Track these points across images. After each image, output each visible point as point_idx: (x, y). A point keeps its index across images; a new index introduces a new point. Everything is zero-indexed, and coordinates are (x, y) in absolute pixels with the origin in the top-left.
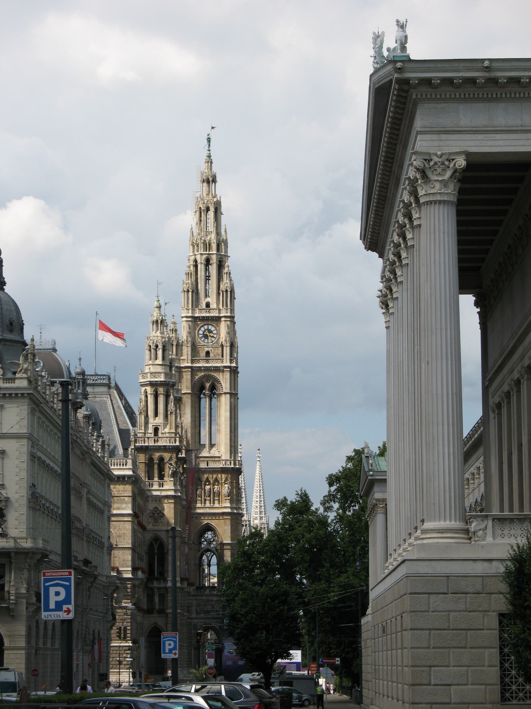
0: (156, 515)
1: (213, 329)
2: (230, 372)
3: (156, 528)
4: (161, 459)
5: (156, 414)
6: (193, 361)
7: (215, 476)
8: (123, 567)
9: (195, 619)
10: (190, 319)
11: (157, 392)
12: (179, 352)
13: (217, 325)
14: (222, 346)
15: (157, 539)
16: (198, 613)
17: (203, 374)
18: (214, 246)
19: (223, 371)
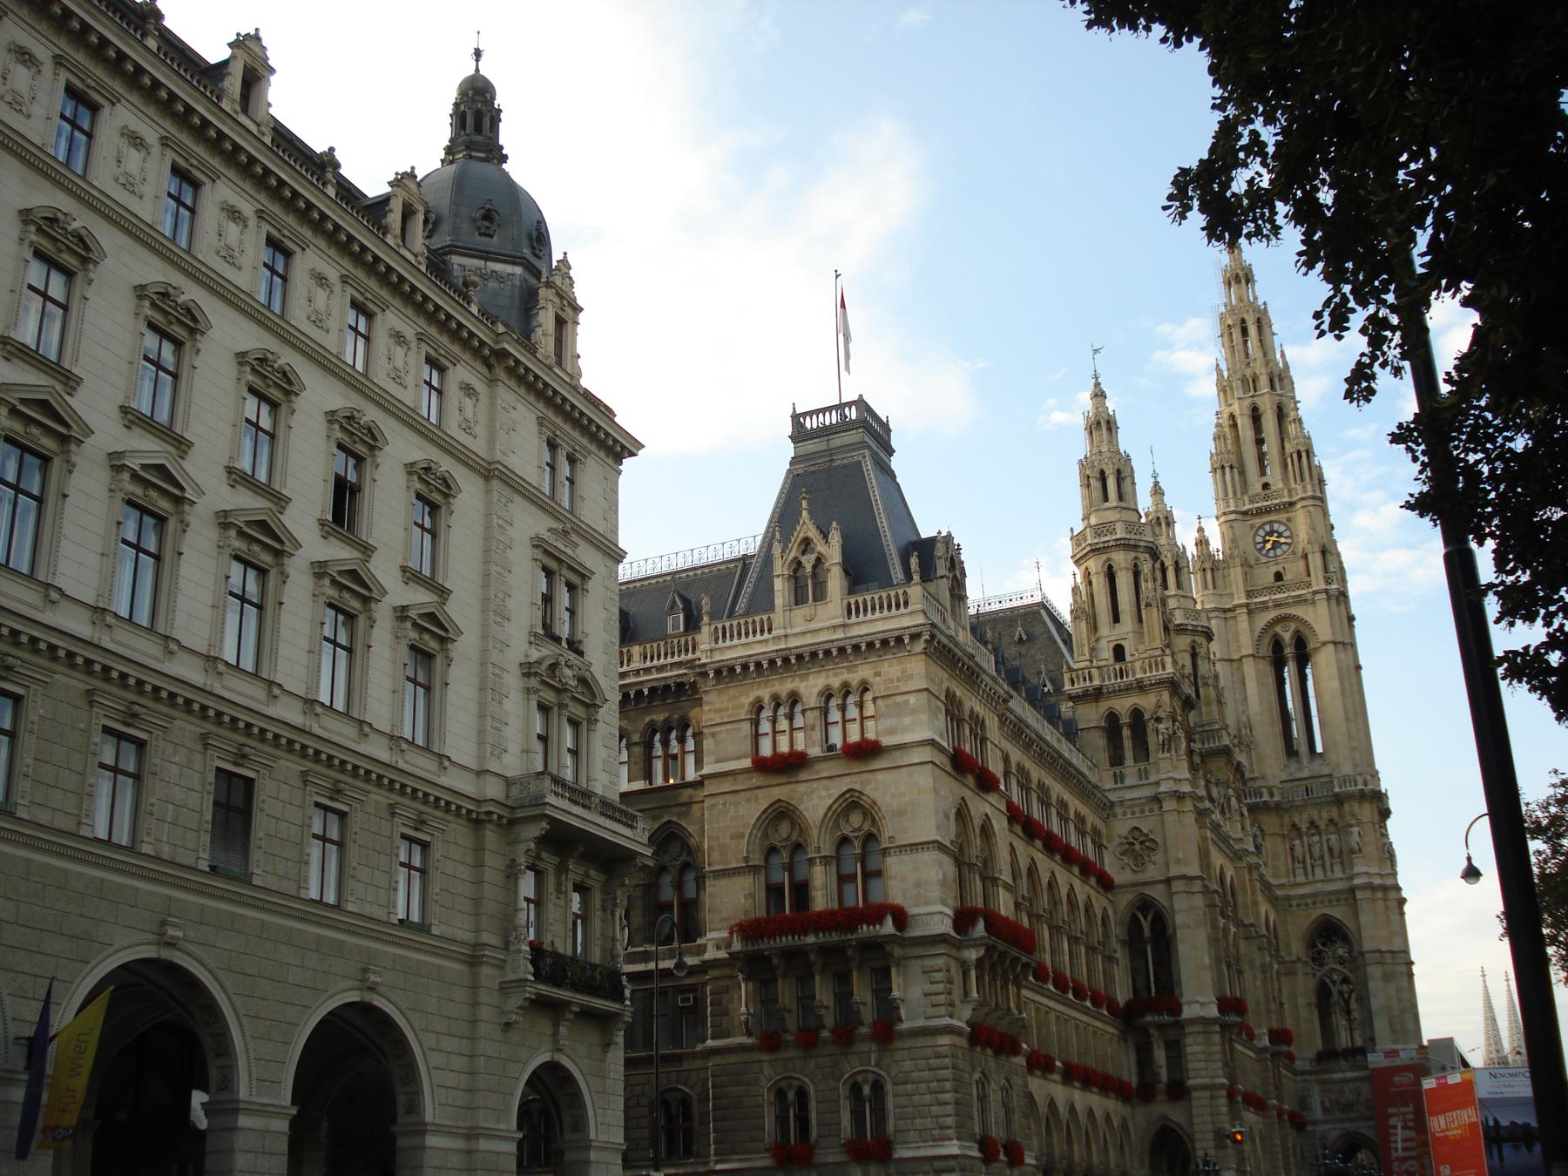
0: (1137, 847)
1: (1282, 529)
2: (1328, 599)
3: (1141, 877)
4: (1137, 713)
5: (1116, 618)
6: (1249, 594)
7: (1325, 815)
8: (916, 905)
9: (1324, 1122)
10: (1233, 516)
11: (1110, 567)
12: (1219, 582)
13: (1289, 519)
14: (1305, 556)
15: (1144, 904)
16: (1325, 1109)
17: (1272, 615)
18: (1264, 381)
19: (1314, 602)
